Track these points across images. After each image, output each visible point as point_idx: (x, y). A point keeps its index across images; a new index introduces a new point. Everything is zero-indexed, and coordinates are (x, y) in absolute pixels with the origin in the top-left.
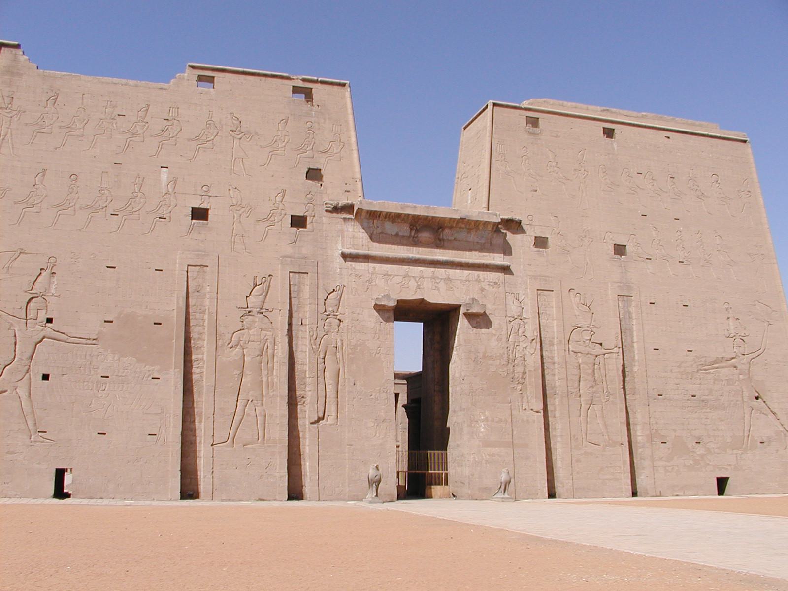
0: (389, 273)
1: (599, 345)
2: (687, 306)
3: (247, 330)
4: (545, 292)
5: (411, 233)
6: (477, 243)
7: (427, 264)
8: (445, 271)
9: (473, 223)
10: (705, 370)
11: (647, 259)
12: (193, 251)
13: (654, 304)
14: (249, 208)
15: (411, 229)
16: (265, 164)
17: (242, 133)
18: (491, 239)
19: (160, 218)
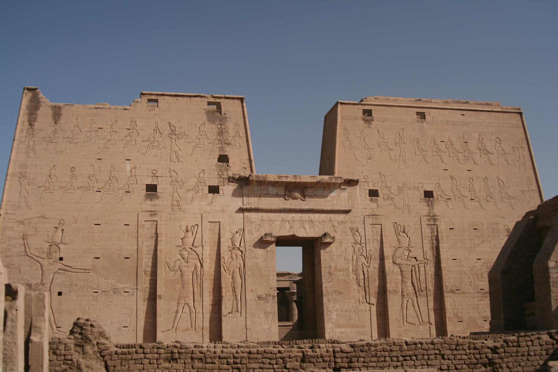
3: (182, 260)
5: (285, 193)
12: (148, 212)
15: (286, 190)
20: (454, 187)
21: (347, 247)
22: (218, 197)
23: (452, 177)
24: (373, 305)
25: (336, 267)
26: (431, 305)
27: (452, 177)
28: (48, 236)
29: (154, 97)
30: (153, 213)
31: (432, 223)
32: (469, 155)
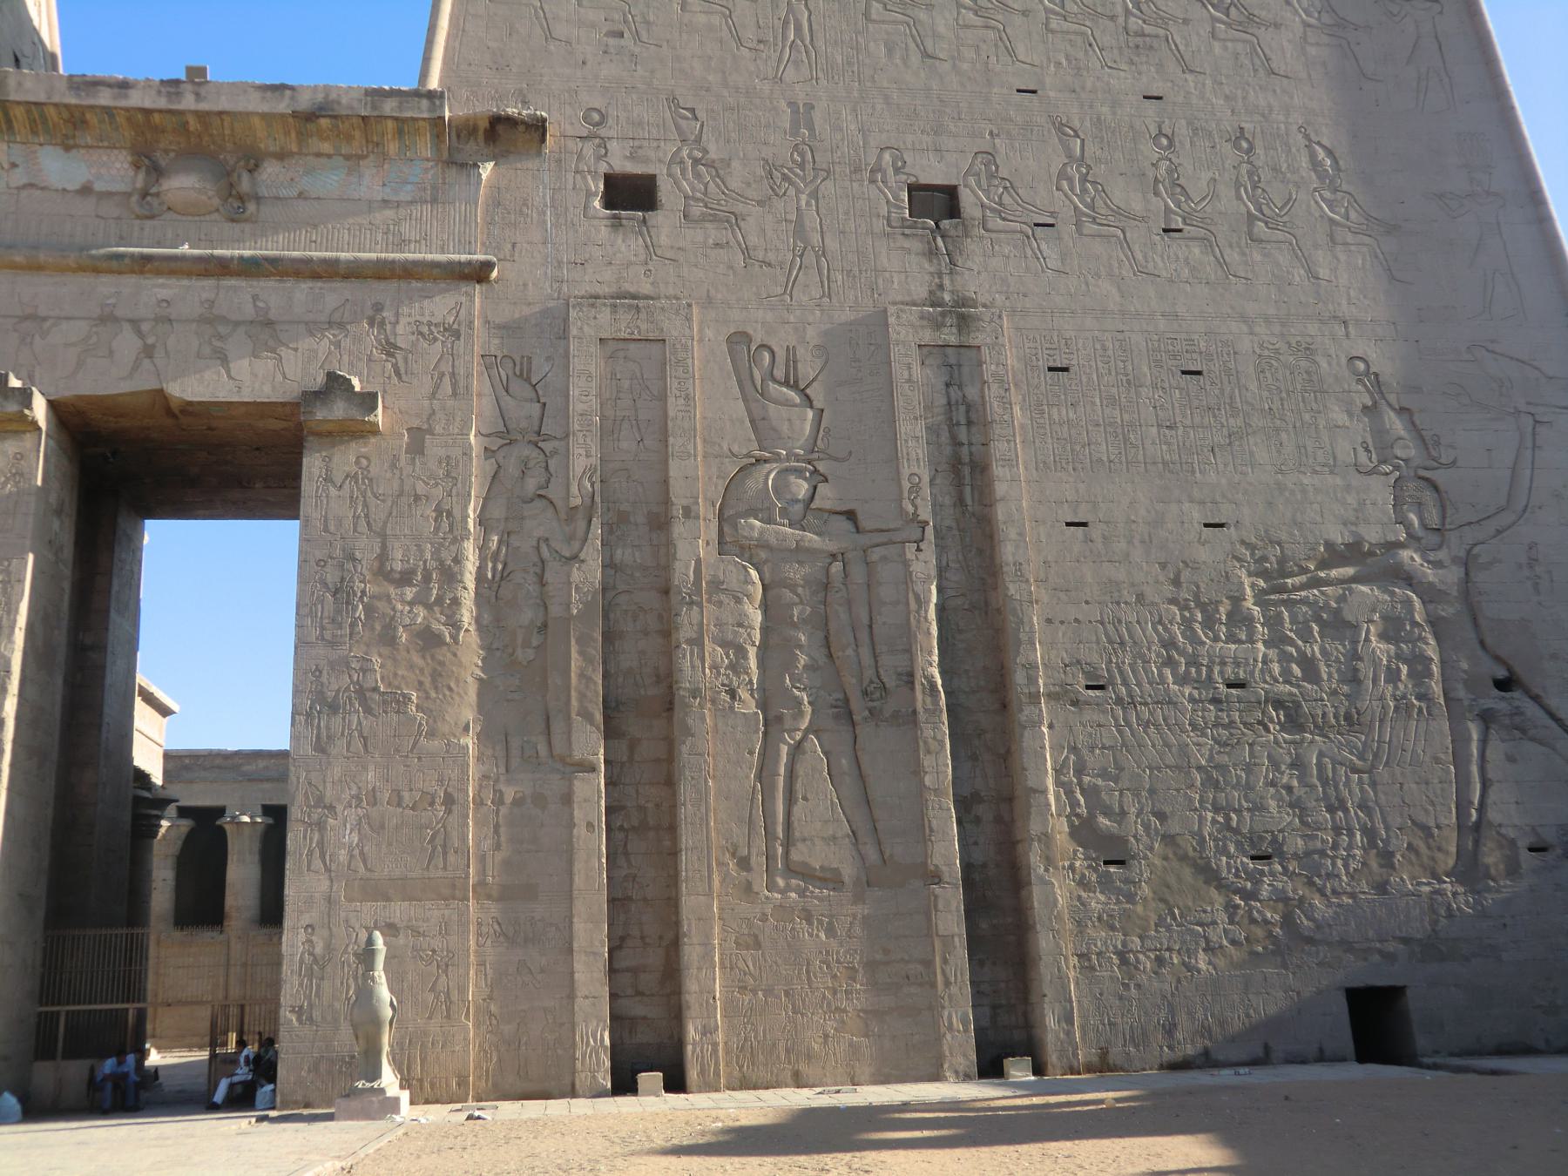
0: (42, 312)
1: (843, 518)
2: (1199, 373)
4: (632, 346)
5: (134, 183)
6: (384, 201)
7: (189, 274)
8: (255, 298)
9: (357, 134)
10: (1282, 589)
11: (1037, 225)
13: (1065, 369)
15: (137, 166)
18: (434, 188)
20: (1072, 171)
21: (456, 452)
23: (1060, 127)
24: (593, 769)
25: (383, 557)
26: (941, 767)
27: (1060, 127)
31: (950, 336)
32: (1148, 29)
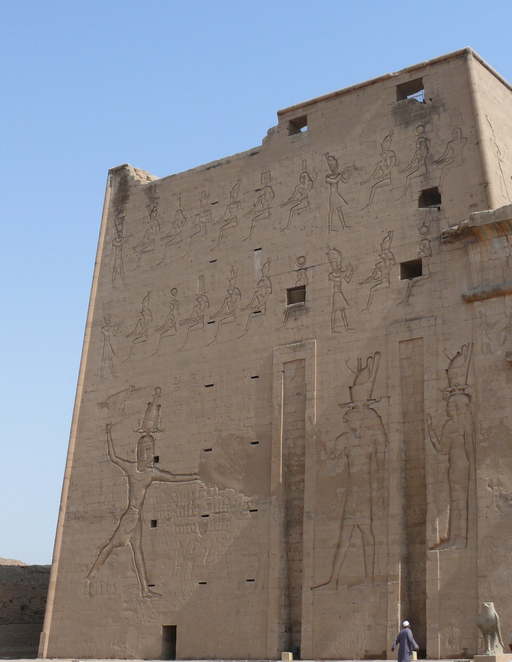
14: (350, 269)
16: (368, 205)
17: (339, 174)
19: (255, 313)
22: (420, 283)
28: (139, 420)
29: (299, 114)
30: (300, 344)
